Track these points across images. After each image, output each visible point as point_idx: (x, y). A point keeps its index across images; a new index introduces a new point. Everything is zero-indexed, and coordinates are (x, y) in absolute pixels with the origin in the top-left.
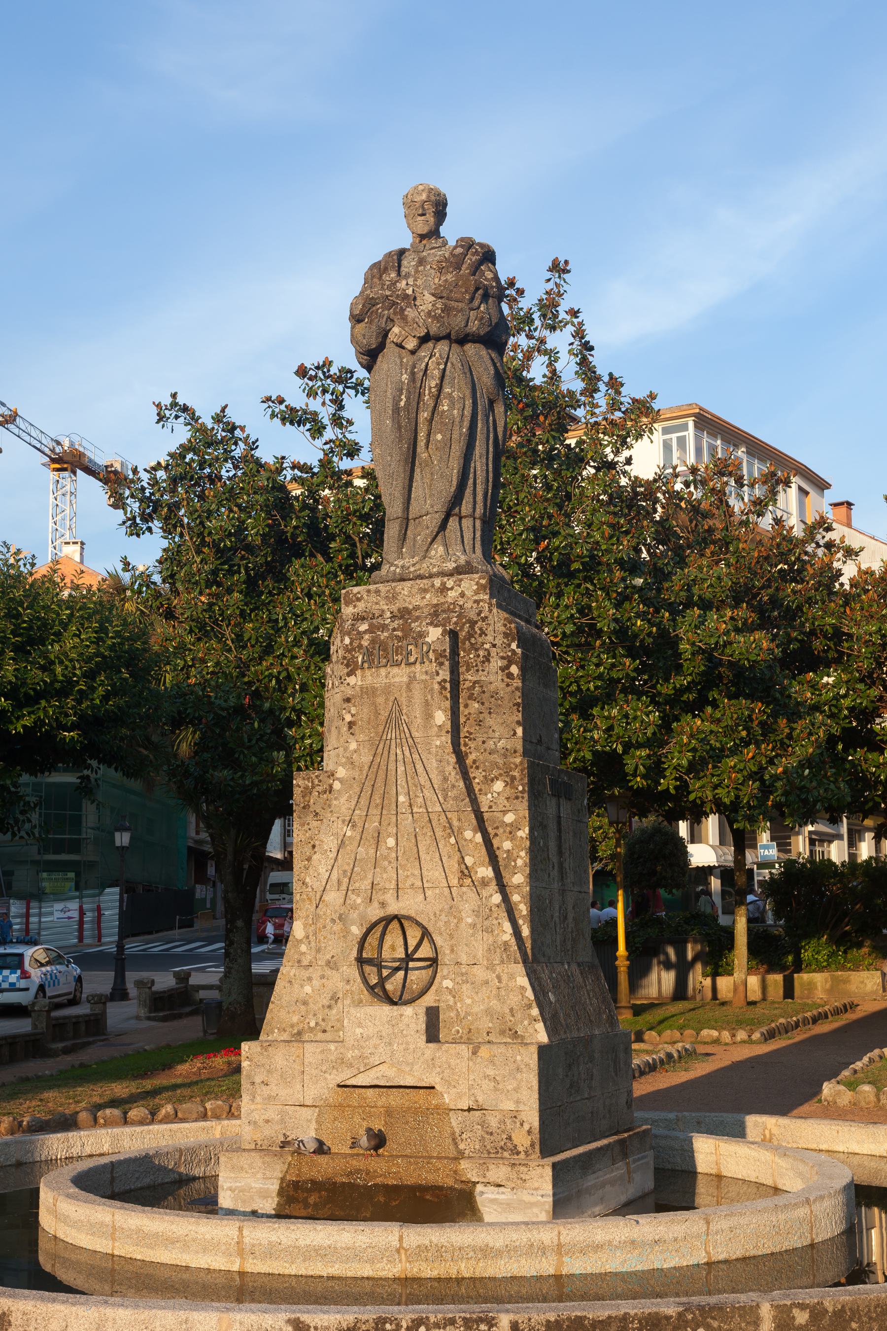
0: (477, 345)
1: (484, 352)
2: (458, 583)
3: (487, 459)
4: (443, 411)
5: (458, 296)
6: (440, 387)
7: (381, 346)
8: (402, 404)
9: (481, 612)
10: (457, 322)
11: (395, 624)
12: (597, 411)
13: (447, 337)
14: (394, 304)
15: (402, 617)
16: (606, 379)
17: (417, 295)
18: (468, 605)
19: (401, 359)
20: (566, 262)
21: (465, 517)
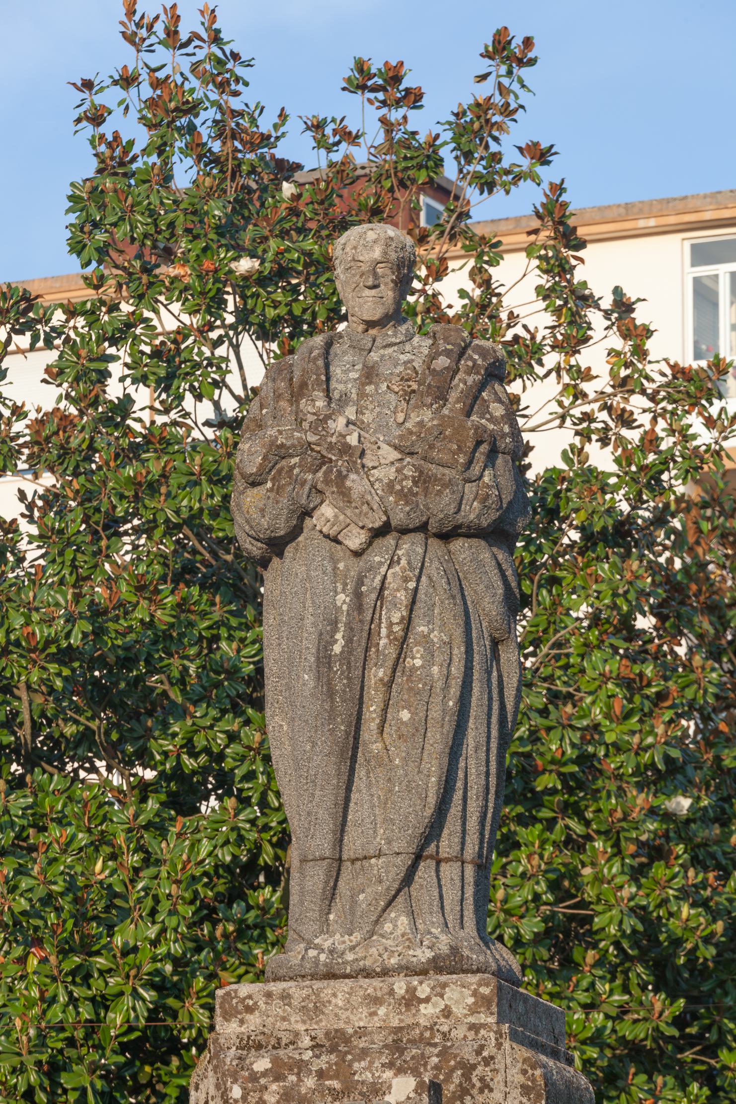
0: (475, 542)
1: (485, 555)
2: (440, 990)
3: (488, 750)
4: (414, 669)
5: (445, 457)
6: (408, 623)
7: (295, 532)
8: (337, 649)
9: (482, 1047)
10: (441, 506)
11: (323, 1062)
12: (589, 388)
13: (423, 528)
14: (324, 460)
15: (333, 1049)
16: (607, 303)
17: (367, 445)
18: (459, 1033)
19: (334, 561)
20: (528, 42)
21: (447, 860)
